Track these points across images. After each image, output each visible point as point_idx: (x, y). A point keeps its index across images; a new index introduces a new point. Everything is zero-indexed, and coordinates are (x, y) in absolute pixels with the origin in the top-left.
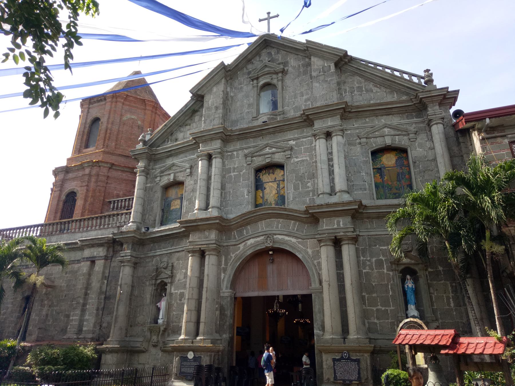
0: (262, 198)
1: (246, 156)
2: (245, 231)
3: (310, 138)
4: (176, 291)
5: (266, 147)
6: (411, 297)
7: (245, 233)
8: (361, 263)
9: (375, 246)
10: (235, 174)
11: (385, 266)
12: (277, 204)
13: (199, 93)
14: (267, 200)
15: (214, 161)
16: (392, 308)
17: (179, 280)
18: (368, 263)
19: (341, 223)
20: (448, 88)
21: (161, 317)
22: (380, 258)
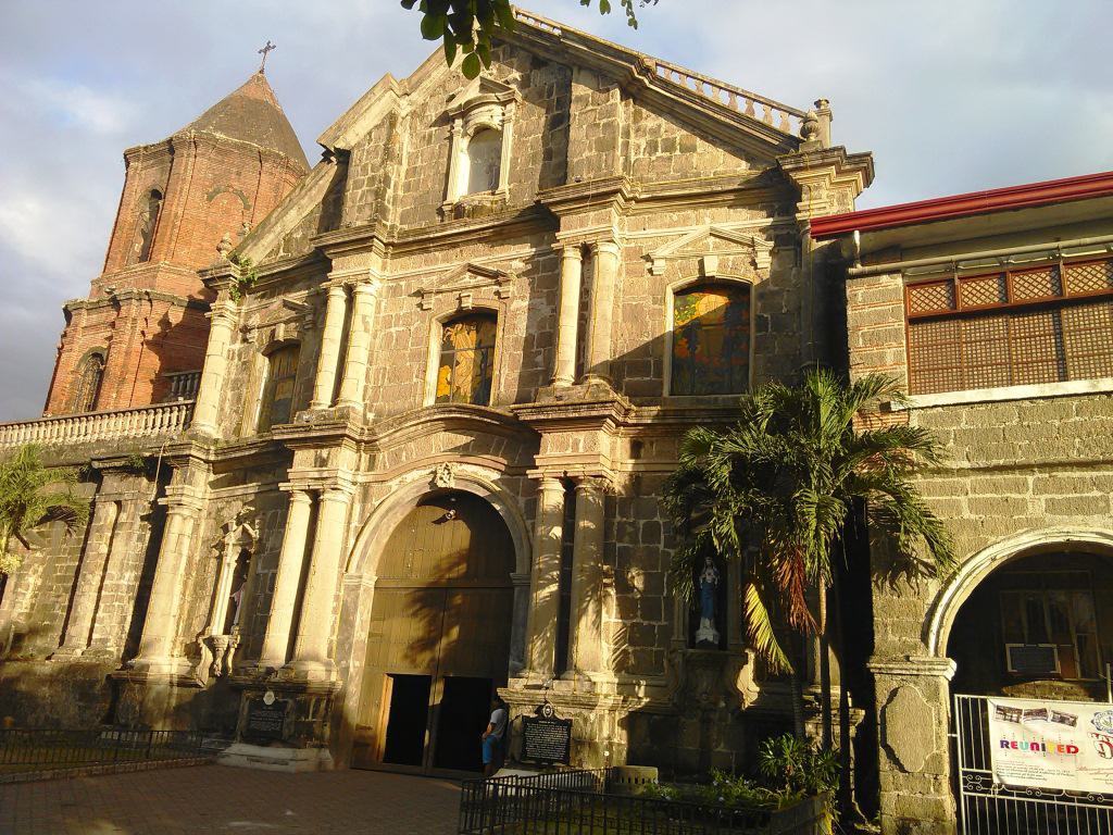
0: (449, 383)
1: (420, 294)
2: (404, 454)
3: (552, 256)
4: (266, 571)
5: (461, 273)
6: (708, 602)
7: (404, 458)
8: (615, 527)
9: (650, 494)
10: (397, 329)
11: (662, 537)
12: (475, 400)
13: (341, 145)
14: (458, 388)
15: (359, 299)
16: (663, 623)
17: (271, 550)
18: (630, 529)
19: (581, 445)
20: (842, 149)
21: (236, 621)
22: (656, 519)
